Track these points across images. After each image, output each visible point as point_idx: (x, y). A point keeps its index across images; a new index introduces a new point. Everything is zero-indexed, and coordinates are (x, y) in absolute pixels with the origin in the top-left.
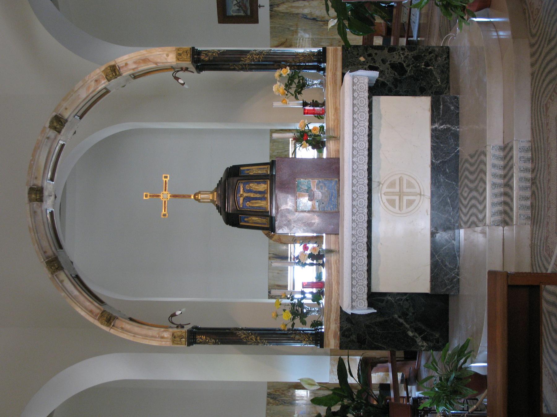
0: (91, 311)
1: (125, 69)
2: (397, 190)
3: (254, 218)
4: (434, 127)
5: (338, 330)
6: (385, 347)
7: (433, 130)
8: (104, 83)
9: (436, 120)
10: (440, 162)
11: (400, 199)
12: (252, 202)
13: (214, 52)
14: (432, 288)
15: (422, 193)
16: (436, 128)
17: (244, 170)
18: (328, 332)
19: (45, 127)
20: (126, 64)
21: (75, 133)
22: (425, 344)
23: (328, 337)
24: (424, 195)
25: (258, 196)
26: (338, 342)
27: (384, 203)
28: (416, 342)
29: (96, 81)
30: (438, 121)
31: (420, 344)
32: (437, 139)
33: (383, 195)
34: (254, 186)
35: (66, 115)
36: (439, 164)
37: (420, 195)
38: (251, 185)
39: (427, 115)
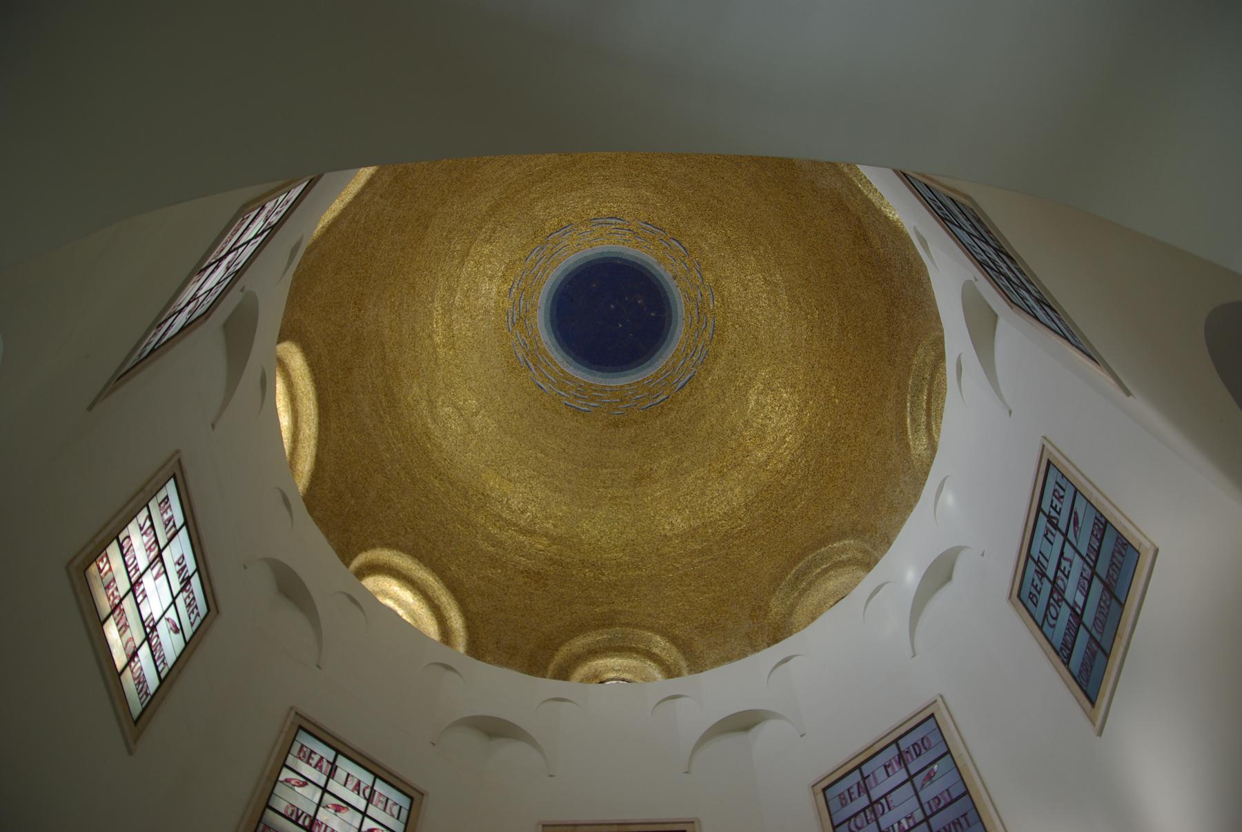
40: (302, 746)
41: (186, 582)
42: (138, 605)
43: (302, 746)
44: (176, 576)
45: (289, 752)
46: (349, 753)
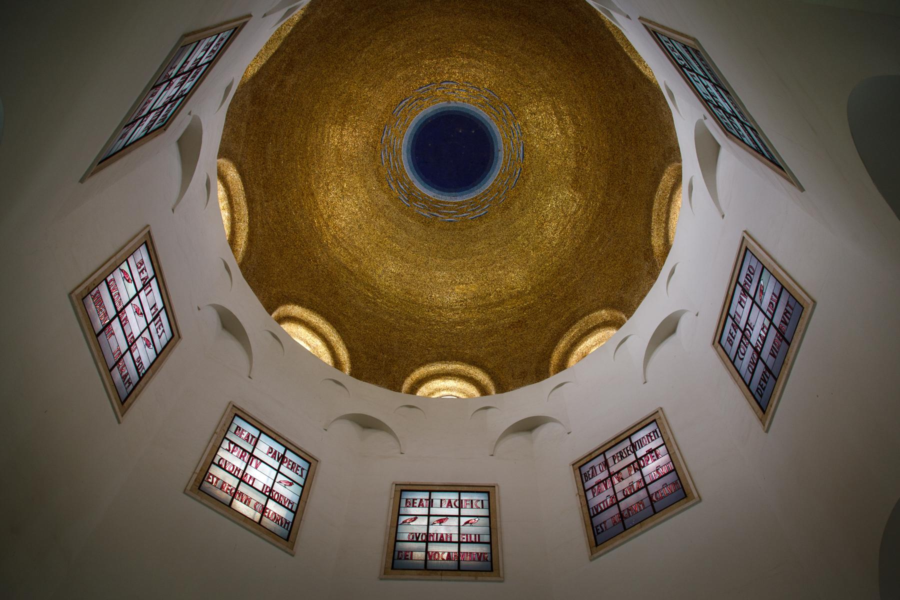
41: (282, 459)
42: (251, 486)
44: (272, 459)
46: (438, 488)
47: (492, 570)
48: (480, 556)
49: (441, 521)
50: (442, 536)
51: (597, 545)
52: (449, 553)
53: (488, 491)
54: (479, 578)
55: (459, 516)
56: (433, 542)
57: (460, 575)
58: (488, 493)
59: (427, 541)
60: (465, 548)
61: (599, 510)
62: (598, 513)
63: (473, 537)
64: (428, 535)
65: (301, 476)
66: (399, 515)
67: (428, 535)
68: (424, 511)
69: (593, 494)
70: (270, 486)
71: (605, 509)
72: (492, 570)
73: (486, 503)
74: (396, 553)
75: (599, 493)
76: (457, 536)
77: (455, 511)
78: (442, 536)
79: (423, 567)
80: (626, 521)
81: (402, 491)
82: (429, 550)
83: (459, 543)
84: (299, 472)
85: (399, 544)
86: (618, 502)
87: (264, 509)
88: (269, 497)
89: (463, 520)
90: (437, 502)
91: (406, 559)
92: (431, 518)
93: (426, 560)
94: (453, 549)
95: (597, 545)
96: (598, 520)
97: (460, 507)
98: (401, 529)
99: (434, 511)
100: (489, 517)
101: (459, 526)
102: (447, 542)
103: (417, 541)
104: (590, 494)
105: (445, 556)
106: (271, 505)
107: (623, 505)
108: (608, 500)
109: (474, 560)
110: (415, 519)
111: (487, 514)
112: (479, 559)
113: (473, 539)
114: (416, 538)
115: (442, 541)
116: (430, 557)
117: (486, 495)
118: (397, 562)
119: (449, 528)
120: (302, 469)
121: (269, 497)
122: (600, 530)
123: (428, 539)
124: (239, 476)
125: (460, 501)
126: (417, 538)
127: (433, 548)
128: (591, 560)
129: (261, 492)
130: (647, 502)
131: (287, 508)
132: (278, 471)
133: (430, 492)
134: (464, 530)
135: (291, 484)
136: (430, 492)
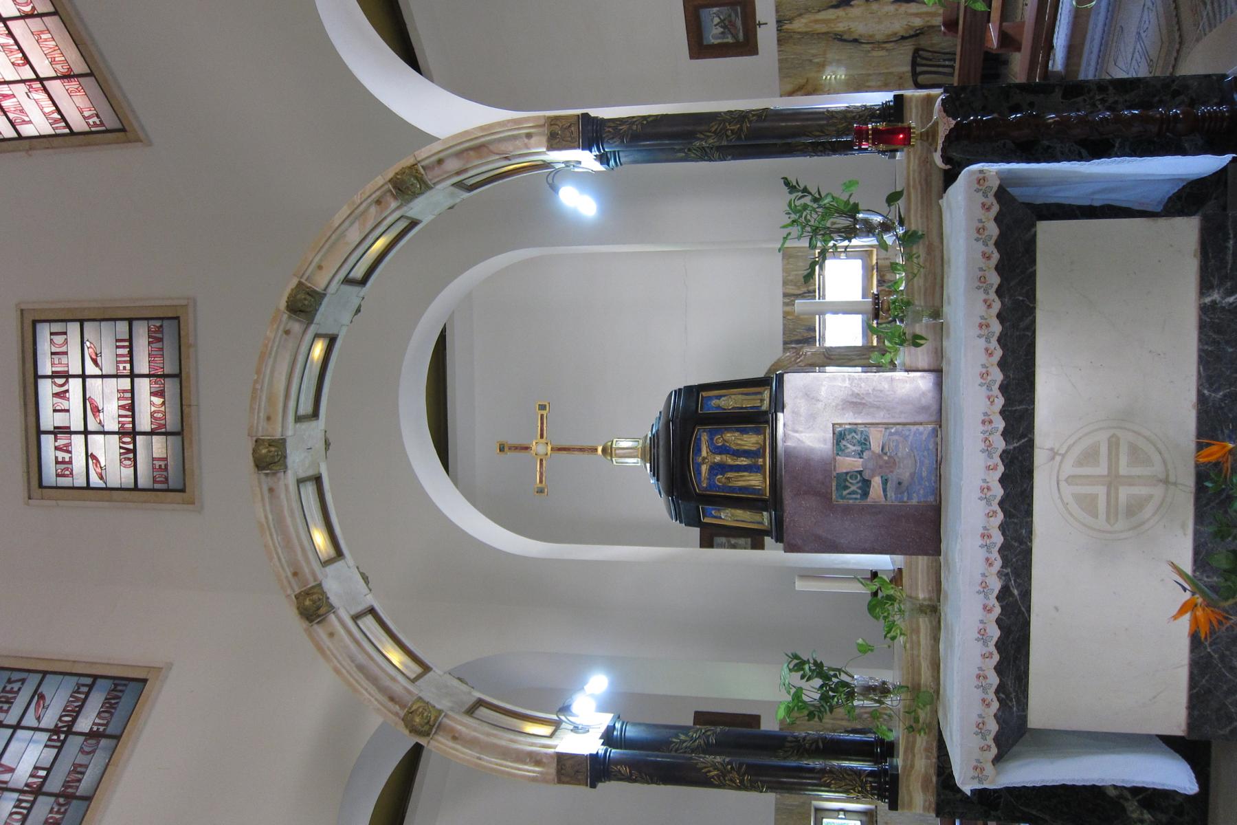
0: (392, 699)
1: (437, 171)
2: (1102, 469)
3: (740, 513)
4: (1208, 300)
5: (932, 771)
6: (1047, 818)
7: (1204, 310)
8: (398, 208)
9: (1216, 282)
10: (1225, 396)
11: (1108, 494)
12: (729, 475)
13: (633, 123)
14: (1194, 720)
15: (1172, 479)
16: (1214, 302)
17: (710, 398)
18: (909, 775)
19: (278, 310)
20: (440, 162)
21: (358, 311)
22: (1147, 816)
23: (908, 786)
24: (1175, 484)
25: (743, 461)
26: (932, 799)
27: (1066, 505)
28: (1124, 809)
29: (378, 202)
30: (1219, 286)
31: (1135, 816)
32: (1219, 332)
33: (1063, 484)
34: (732, 438)
35: (320, 283)
36: (1222, 400)
37: (1166, 482)
38: (728, 436)
39: (1190, 268)
40: (58, 475)
42: (49, 770)
43: (58, 475)
45: (73, 488)
47: (177, 318)
48: (155, 338)
49: (96, 411)
50: (119, 407)
51: (123, 130)
52: (153, 394)
53: (31, 323)
54: (191, 340)
55: (84, 377)
56: (133, 422)
57: (188, 377)
58: (35, 323)
59: (134, 433)
60: (142, 366)
61: (56, 116)
62: (63, 119)
63: (120, 351)
64: (121, 433)
65: (23, 681)
66: (88, 487)
67: (121, 433)
68: (78, 441)
69: (24, 122)
70: (45, 736)
71: (54, 104)
72: (177, 318)
73: (57, 327)
74: (157, 486)
75: (22, 111)
76: (120, 380)
77: (75, 385)
78: (122, 407)
79: (179, 438)
80: (76, 71)
81: (41, 486)
82: (148, 429)
83: (132, 376)
84: (16, 686)
85: (141, 484)
86: (39, 79)
87: (92, 735)
88: (70, 732)
89: (91, 369)
90: (60, 420)
91: (166, 469)
92: (90, 428)
93: (166, 434)
94: (143, 386)
95: (123, 130)
96: (78, 124)
97: (67, 376)
98: (113, 482)
99: (77, 425)
100: (82, 322)
101: (102, 376)
102: (133, 398)
103: (134, 451)
104: (27, 130)
105: (157, 400)
106: (84, 724)
107: (45, 70)
108: (35, 95)
109: (162, 349)
110: (94, 457)
111: (78, 324)
112: (160, 340)
113: (125, 351)
114: (130, 454)
115: (132, 408)
116: (161, 426)
117: (39, 326)
118: (171, 486)
119: (108, 395)
120: (9, 681)
121: (70, 732)
122: (95, 119)
123: (129, 433)
124: (31, 798)
125: (55, 375)
126: (128, 451)
127: (144, 423)
128: (150, 144)
129: (60, 749)
130: (35, 24)
131: (87, 695)
132: (17, 727)
133: (39, 432)
134: (108, 368)
135: (42, 697)
136: (39, 432)
